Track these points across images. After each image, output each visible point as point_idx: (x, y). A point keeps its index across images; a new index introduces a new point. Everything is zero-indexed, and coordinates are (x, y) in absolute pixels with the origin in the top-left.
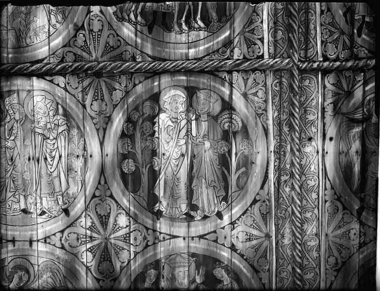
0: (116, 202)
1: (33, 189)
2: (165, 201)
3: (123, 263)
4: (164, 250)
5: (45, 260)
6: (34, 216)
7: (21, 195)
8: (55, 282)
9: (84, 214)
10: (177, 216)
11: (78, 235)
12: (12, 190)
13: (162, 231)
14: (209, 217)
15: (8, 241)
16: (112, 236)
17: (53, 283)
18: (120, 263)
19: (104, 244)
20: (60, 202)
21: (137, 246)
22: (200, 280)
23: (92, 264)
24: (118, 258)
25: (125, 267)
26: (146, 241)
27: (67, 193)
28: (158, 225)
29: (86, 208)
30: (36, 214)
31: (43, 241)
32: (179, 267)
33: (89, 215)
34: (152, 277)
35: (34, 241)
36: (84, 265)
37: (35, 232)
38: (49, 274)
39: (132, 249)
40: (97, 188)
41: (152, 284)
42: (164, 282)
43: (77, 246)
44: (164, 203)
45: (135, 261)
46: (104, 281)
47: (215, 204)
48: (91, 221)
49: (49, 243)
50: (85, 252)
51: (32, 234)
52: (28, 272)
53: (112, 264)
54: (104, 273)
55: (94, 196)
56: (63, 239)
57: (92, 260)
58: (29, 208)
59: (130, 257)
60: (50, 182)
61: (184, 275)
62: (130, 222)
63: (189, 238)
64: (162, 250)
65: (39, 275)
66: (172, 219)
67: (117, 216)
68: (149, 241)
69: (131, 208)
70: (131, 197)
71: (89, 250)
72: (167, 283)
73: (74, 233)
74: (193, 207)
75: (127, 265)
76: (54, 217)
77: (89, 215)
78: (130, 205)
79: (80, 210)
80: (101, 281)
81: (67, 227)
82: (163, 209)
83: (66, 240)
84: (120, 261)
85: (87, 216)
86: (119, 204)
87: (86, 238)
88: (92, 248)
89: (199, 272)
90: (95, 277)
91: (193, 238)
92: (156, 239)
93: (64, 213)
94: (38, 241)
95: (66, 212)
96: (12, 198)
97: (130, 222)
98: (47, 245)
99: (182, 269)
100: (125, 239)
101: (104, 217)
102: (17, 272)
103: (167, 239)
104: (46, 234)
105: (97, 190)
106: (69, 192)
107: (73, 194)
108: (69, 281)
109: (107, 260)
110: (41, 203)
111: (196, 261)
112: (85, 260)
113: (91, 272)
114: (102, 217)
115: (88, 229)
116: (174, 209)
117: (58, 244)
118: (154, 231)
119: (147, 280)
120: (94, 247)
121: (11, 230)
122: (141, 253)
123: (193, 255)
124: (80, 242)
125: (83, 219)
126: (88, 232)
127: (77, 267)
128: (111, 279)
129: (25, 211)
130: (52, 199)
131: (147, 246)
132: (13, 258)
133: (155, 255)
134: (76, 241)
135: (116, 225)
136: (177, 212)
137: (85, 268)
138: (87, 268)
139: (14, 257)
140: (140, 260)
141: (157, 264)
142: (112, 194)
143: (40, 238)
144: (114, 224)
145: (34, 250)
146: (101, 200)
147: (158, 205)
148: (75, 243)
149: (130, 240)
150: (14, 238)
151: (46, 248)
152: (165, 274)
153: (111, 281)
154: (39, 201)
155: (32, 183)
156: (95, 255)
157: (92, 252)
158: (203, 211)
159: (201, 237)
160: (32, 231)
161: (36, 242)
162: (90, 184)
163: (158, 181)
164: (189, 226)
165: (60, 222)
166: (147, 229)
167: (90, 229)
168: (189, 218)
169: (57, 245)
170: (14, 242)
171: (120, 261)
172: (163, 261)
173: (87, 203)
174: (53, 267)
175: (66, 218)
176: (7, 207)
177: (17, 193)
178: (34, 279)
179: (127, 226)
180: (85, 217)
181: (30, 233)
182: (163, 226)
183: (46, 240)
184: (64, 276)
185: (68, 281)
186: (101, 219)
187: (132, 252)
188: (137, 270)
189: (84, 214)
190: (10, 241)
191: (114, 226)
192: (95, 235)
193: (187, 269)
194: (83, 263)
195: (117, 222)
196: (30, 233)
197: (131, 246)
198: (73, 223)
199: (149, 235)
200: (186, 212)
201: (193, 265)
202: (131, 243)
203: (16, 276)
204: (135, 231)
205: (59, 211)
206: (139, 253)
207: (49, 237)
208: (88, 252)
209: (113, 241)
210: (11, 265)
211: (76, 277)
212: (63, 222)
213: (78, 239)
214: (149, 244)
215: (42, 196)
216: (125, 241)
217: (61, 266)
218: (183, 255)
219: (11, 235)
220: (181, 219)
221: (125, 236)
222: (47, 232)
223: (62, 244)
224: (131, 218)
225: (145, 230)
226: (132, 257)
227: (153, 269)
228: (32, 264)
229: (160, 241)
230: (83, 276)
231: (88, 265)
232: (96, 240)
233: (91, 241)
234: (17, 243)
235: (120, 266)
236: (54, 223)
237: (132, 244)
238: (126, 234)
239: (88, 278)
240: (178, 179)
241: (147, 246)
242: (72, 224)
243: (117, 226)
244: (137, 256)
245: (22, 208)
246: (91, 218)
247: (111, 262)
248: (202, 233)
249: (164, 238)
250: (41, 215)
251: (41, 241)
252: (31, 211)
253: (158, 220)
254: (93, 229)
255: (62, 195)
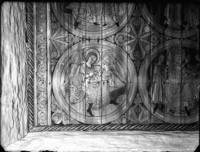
0: (144, 19)
1: (100, 11)
2: (169, 19)
3: (147, 51)
4: (169, 46)
5: (105, 49)
6: (101, 26)
7: (94, 16)
8: (110, 61)
9: (127, 25)
10: (176, 27)
11: (123, 36)
12: (89, 13)
13: (168, 35)
14: (193, 28)
15: (86, 39)
16: (141, 37)
17: (110, 62)
18: (145, 52)
19: (137, 41)
20: (115, 19)
21: (154, 43)
22: (188, 61)
23: (131, 52)
24: (144, 49)
25: (147, 54)
26: (159, 40)
27: (118, 14)
28: (166, 32)
29: (128, 23)
30: (101, 25)
31: (105, 39)
32: (177, 54)
33: (129, 26)
34: (162, 60)
35: (100, 39)
36: (127, 53)
37: (101, 35)
38: (107, 57)
39: (152, 45)
40: (134, 12)
41: (162, 63)
42: (168, 62)
43: (123, 43)
44: (169, 20)
45: (153, 51)
46: (136, 61)
47: (196, 21)
48: (130, 29)
49: (108, 41)
50: (127, 45)
51: (99, 36)
52: (96, 56)
53: (141, 52)
54: (136, 57)
55: (132, 16)
56: (115, 39)
57: (131, 50)
58: (98, 22)
59: (151, 48)
60: (109, 9)
61: (179, 58)
62: (151, 30)
63: (181, 39)
64: (168, 45)
65: (102, 58)
66: (173, 29)
67: (144, 27)
68: (160, 40)
69: (152, 23)
70: (152, 17)
71: (129, 44)
72: (170, 63)
73: (121, 36)
74: (184, 23)
75: (149, 52)
76: (111, 27)
77: (129, 26)
78: (151, 21)
79: (124, 24)
80: (134, 62)
81: (118, 33)
82: (168, 23)
83: (117, 39)
84: (145, 51)
85: (128, 26)
86: (145, 20)
87: (128, 38)
88: (130, 44)
89: (187, 57)
90: (131, 59)
91: (184, 39)
92: (164, 39)
93: (116, 25)
94: (102, 39)
95: (117, 24)
96: (89, 17)
97: (151, 30)
98: (107, 42)
99: (178, 55)
100: (148, 39)
101: (137, 27)
102: (90, 56)
103: (171, 39)
104: (106, 36)
105: (134, 13)
106: (119, 14)
107: (121, 15)
108: (118, 61)
109: (138, 50)
110: (104, 19)
111: (185, 51)
112: (127, 50)
113: (130, 57)
114: (136, 27)
115: (129, 33)
116: (174, 23)
117: (113, 41)
118: (164, 35)
119: (160, 61)
120: (132, 43)
121: (88, 34)
122: (156, 46)
123: (184, 48)
124: (124, 40)
125: (126, 28)
126: (129, 35)
127: (122, 53)
128: (139, 60)
129: (96, 24)
130: (110, 17)
131: (160, 43)
132: (89, 48)
133: (164, 47)
134: (122, 40)
135: (143, 32)
136: (176, 25)
137: (126, 54)
138: (128, 54)
139: (89, 48)
140: (156, 50)
141: (165, 53)
142: (142, 15)
143: (104, 38)
144: (142, 31)
145: (100, 44)
146: (136, 18)
147: (166, 21)
148: (121, 41)
149: (150, 39)
150: (89, 38)
151: (106, 43)
152: (169, 58)
153: (140, 61)
154: (103, 18)
155: (100, 9)
156: (132, 48)
157: (131, 45)
158: (190, 24)
159: (188, 38)
160: (99, 34)
161: (101, 40)
162: (131, 9)
163: (166, 9)
164: (182, 33)
165: (114, 30)
166: (160, 34)
167: (130, 33)
168: (182, 29)
169: (112, 42)
170: (89, 40)
171: (145, 51)
172: (168, 51)
173: (129, 20)
174: (110, 53)
175: (117, 28)
176: (87, 21)
177: (92, 14)
178: (100, 60)
179: (149, 32)
180: (127, 27)
181: (98, 35)
182: (168, 32)
183: (106, 39)
184: (115, 59)
185: (117, 61)
186: (136, 28)
187: (152, 46)
188: (154, 55)
189: (127, 25)
190: (88, 39)
191: (143, 32)
192: (132, 37)
193: (180, 55)
194: (125, 51)
195: (144, 30)
196: (98, 35)
197: (151, 43)
198: (121, 30)
199: (161, 37)
200: (180, 25)
201: (184, 53)
202: (151, 41)
203: (90, 58)
204: (153, 35)
205: (114, 23)
206: (155, 46)
207: (108, 38)
208: (128, 46)
209: (141, 40)
210: (87, 52)
211: (122, 59)
212: (116, 29)
213: (123, 39)
214: (161, 41)
215: (105, 16)
216: (148, 40)
217: (114, 53)
218: (179, 48)
219: (88, 36)
220: (178, 28)
221: (148, 37)
222: (107, 35)
223: (115, 41)
224: (151, 28)
225: (159, 35)
226: (151, 49)
227: (163, 55)
228: (98, 52)
229: (167, 40)
230: (125, 58)
231: (129, 52)
232: (132, 39)
233: (130, 40)
234: (91, 41)
235: (145, 53)
236: (111, 30)
237: (152, 42)
238: (149, 36)
239: (128, 60)
240: (176, 8)
241: (160, 43)
242: (120, 31)
243: (144, 32)
244: (154, 48)
245: (94, 22)
246: (130, 28)
247: (140, 51)
248: (189, 36)
249: (169, 39)
250: (104, 26)
251: (104, 39)
252: (99, 24)
253: (166, 29)
254: (131, 33)
255: (116, 16)
